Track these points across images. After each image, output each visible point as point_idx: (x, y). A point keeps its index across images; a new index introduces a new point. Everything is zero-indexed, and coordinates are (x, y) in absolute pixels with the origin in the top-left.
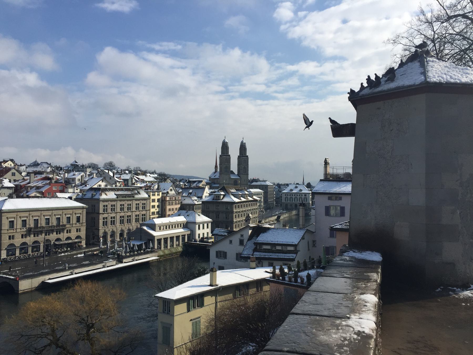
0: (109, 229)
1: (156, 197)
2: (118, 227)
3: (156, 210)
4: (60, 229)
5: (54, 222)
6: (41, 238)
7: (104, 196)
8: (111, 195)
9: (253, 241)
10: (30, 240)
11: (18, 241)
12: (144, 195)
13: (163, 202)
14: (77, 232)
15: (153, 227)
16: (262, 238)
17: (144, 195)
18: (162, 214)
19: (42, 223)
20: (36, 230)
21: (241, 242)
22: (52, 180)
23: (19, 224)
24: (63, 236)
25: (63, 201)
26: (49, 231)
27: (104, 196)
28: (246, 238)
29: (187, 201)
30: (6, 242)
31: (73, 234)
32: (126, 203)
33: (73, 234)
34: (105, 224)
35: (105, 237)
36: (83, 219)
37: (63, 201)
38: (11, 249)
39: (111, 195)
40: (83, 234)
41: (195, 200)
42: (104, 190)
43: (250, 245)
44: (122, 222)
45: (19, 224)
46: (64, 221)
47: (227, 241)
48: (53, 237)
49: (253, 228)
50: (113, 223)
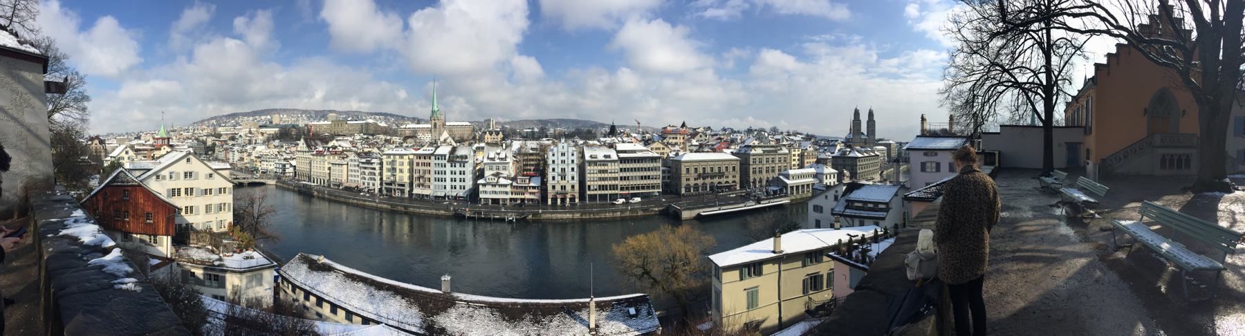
0: (758, 177)
1: (797, 153)
2: (764, 176)
3: (796, 163)
4: (721, 175)
5: (716, 170)
6: (708, 181)
7: (753, 152)
8: (759, 151)
9: (846, 197)
10: (700, 182)
11: (692, 182)
12: (785, 150)
13: (802, 156)
14: (733, 178)
15: (787, 176)
16: (856, 195)
17: (785, 150)
18: (801, 166)
19: (708, 170)
20: (704, 176)
21: (836, 198)
22: (724, 139)
23: (692, 171)
24: (723, 180)
25: (726, 155)
26: (712, 177)
27: (753, 152)
28: (840, 194)
29: (822, 156)
30: (684, 182)
31: (730, 179)
32: (770, 157)
33: (730, 179)
34: (754, 172)
35: (754, 182)
36: (738, 169)
37: (726, 155)
38: (688, 188)
39: (759, 151)
40: (738, 179)
41: (828, 155)
42: (754, 147)
43: (843, 202)
44: (767, 171)
45: (692, 171)
46: (724, 169)
47: (823, 196)
48: (716, 180)
49: (848, 184)
50: (760, 172)
